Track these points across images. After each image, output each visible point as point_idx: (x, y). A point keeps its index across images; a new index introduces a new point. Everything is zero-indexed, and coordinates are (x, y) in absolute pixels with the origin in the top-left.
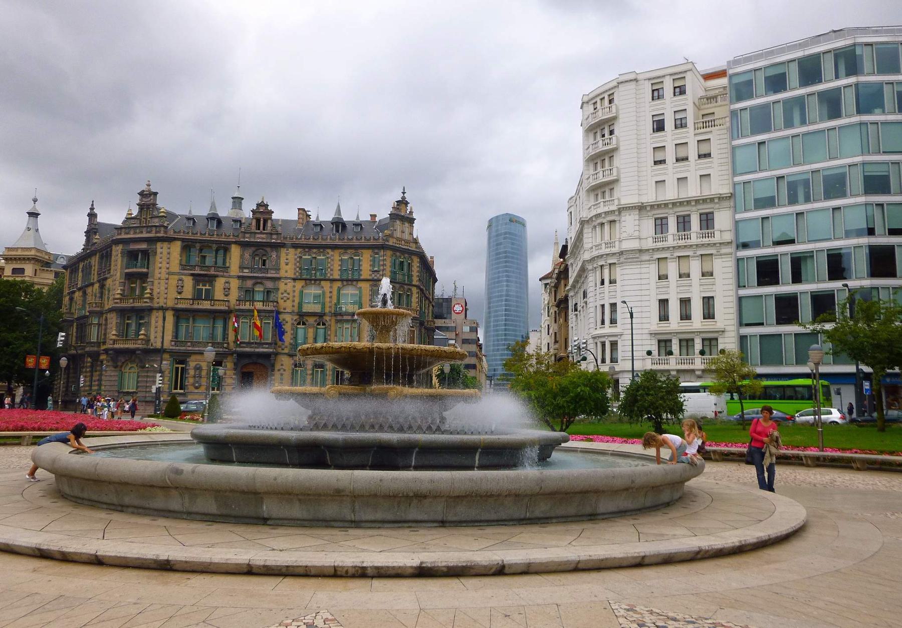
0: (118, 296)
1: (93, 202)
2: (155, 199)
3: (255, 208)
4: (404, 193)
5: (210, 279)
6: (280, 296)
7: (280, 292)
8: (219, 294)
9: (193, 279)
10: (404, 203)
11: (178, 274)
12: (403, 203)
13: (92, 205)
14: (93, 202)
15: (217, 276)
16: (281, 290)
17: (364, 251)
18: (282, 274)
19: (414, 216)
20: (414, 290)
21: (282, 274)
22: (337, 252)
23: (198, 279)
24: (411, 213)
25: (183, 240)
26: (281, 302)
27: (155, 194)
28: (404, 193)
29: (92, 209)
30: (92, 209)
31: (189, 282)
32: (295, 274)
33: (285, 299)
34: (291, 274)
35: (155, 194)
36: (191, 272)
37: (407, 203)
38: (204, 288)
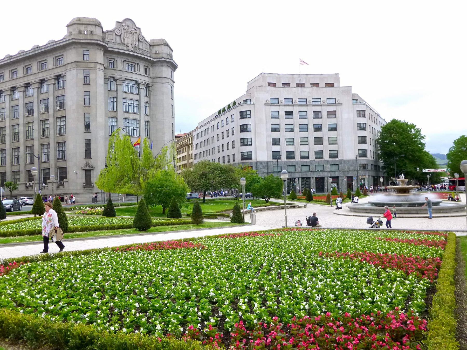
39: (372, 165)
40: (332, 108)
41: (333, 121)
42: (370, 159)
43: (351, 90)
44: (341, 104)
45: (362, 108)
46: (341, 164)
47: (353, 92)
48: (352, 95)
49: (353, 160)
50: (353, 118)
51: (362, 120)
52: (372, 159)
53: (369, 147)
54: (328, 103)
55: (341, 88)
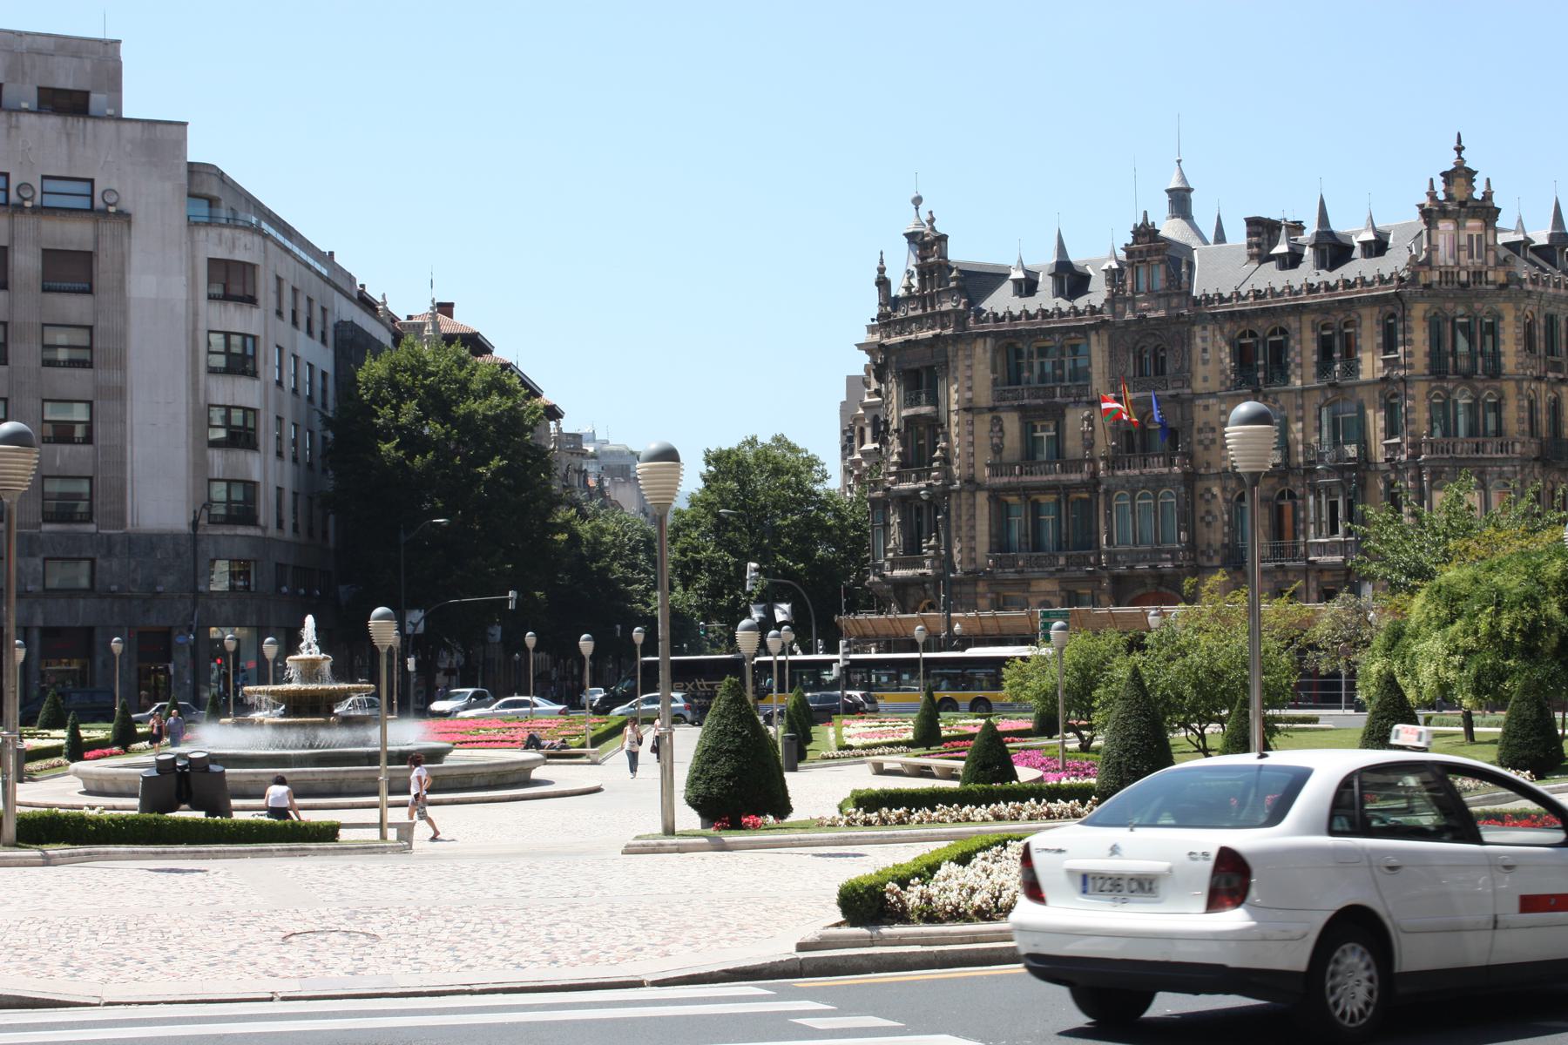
0: (893, 469)
1: (882, 253)
2: (943, 255)
3: (1130, 241)
4: (1459, 149)
5: (1057, 414)
6: (1196, 437)
7: (1196, 426)
8: (1073, 446)
9: (1020, 419)
10: (1460, 176)
11: (991, 409)
12: (1460, 174)
13: (882, 262)
14: (882, 253)
15: (1066, 405)
16: (1199, 422)
17: (1365, 312)
18: (1198, 386)
19: (1497, 201)
20: (1509, 388)
21: (1198, 386)
22: (1307, 319)
23: (1029, 417)
24: (1488, 195)
25: (997, 335)
26: (1199, 449)
27: (943, 239)
28: (1459, 149)
29: (882, 270)
30: (882, 270)
31: (1012, 423)
32: (1222, 383)
33: (1207, 442)
34: (1213, 385)
35: (943, 239)
36: (1016, 403)
37: (1470, 175)
38: (1044, 434)
39: (280, 566)
40: (75, 234)
41: (74, 307)
42: (272, 531)
43: (181, 143)
44: (124, 217)
45: (244, 249)
46: (110, 553)
47: (196, 153)
48: (184, 170)
49: (175, 537)
50: (194, 299)
51: (237, 319)
52: (288, 533)
53: (263, 468)
54: (51, 201)
55: (127, 126)
